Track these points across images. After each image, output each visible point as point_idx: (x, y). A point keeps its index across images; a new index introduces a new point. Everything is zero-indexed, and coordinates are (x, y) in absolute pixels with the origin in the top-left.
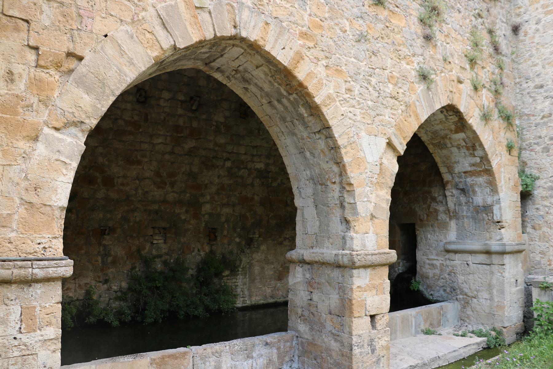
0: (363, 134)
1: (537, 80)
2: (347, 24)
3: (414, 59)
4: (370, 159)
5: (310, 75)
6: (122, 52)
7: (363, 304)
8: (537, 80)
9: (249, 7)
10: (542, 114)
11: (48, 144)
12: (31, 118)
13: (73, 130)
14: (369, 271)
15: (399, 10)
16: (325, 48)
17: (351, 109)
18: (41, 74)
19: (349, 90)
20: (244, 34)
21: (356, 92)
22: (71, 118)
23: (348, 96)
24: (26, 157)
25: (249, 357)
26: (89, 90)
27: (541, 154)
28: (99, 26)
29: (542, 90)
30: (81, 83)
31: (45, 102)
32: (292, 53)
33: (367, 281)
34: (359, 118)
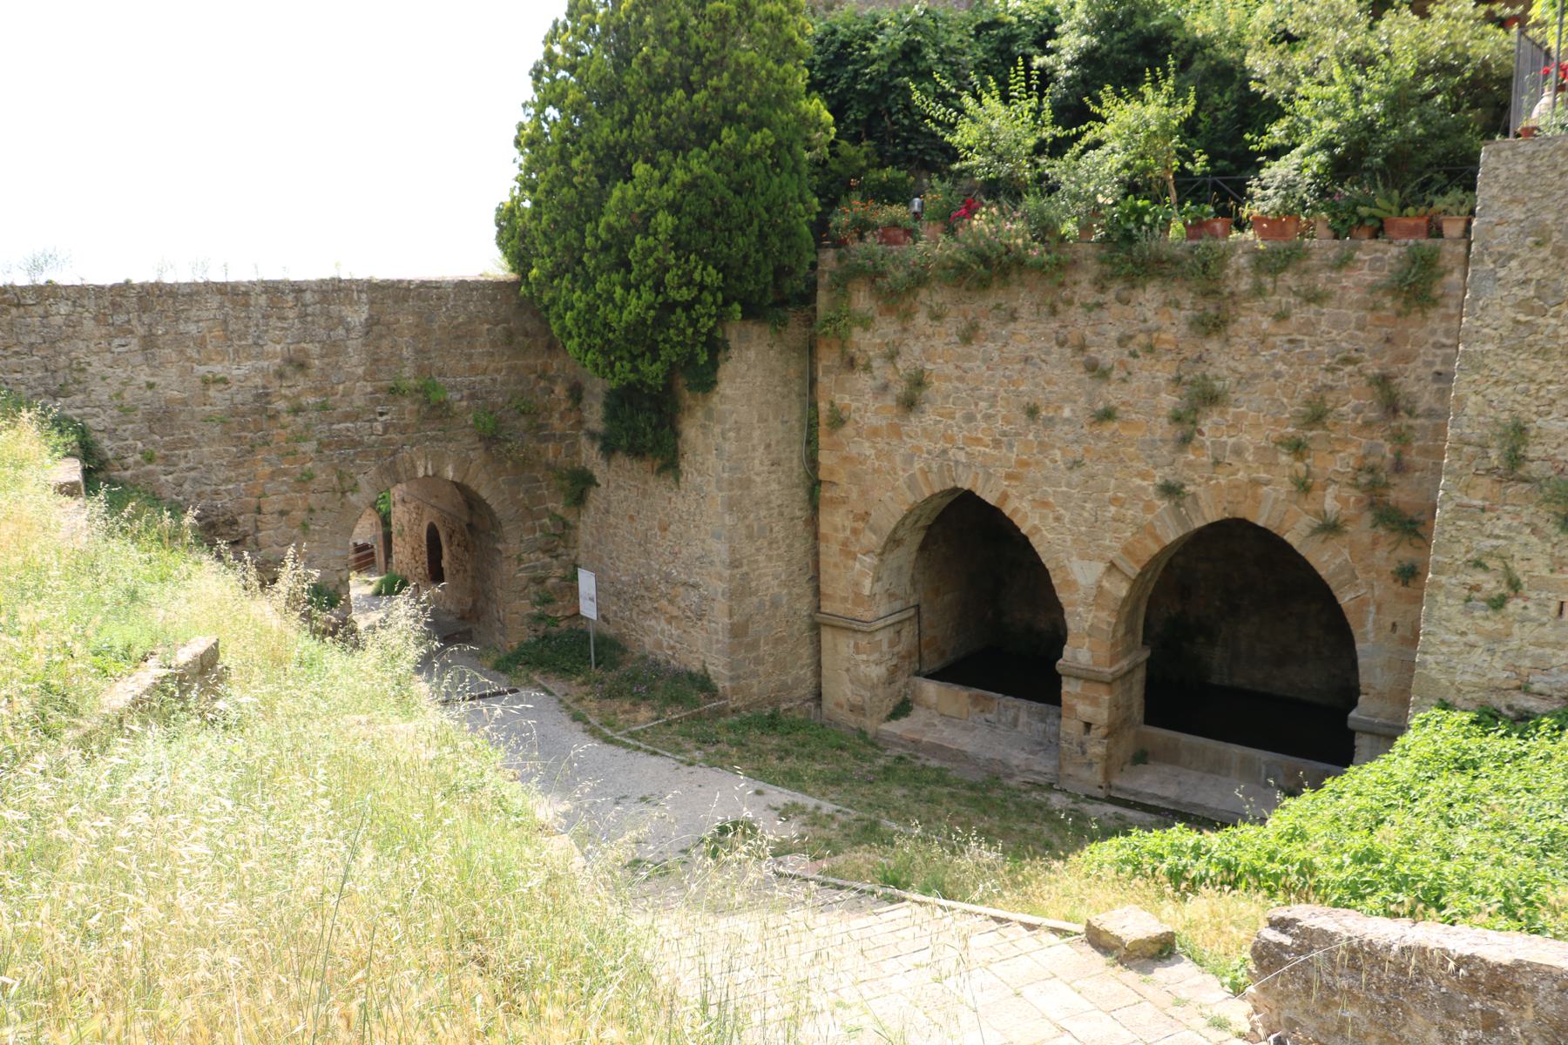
4: (1082, 581)
5: (1016, 510)
7: (1072, 708)
14: (1081, 682)
25: (1043, 721)
26: (875, 533)
33: (1079, 690)
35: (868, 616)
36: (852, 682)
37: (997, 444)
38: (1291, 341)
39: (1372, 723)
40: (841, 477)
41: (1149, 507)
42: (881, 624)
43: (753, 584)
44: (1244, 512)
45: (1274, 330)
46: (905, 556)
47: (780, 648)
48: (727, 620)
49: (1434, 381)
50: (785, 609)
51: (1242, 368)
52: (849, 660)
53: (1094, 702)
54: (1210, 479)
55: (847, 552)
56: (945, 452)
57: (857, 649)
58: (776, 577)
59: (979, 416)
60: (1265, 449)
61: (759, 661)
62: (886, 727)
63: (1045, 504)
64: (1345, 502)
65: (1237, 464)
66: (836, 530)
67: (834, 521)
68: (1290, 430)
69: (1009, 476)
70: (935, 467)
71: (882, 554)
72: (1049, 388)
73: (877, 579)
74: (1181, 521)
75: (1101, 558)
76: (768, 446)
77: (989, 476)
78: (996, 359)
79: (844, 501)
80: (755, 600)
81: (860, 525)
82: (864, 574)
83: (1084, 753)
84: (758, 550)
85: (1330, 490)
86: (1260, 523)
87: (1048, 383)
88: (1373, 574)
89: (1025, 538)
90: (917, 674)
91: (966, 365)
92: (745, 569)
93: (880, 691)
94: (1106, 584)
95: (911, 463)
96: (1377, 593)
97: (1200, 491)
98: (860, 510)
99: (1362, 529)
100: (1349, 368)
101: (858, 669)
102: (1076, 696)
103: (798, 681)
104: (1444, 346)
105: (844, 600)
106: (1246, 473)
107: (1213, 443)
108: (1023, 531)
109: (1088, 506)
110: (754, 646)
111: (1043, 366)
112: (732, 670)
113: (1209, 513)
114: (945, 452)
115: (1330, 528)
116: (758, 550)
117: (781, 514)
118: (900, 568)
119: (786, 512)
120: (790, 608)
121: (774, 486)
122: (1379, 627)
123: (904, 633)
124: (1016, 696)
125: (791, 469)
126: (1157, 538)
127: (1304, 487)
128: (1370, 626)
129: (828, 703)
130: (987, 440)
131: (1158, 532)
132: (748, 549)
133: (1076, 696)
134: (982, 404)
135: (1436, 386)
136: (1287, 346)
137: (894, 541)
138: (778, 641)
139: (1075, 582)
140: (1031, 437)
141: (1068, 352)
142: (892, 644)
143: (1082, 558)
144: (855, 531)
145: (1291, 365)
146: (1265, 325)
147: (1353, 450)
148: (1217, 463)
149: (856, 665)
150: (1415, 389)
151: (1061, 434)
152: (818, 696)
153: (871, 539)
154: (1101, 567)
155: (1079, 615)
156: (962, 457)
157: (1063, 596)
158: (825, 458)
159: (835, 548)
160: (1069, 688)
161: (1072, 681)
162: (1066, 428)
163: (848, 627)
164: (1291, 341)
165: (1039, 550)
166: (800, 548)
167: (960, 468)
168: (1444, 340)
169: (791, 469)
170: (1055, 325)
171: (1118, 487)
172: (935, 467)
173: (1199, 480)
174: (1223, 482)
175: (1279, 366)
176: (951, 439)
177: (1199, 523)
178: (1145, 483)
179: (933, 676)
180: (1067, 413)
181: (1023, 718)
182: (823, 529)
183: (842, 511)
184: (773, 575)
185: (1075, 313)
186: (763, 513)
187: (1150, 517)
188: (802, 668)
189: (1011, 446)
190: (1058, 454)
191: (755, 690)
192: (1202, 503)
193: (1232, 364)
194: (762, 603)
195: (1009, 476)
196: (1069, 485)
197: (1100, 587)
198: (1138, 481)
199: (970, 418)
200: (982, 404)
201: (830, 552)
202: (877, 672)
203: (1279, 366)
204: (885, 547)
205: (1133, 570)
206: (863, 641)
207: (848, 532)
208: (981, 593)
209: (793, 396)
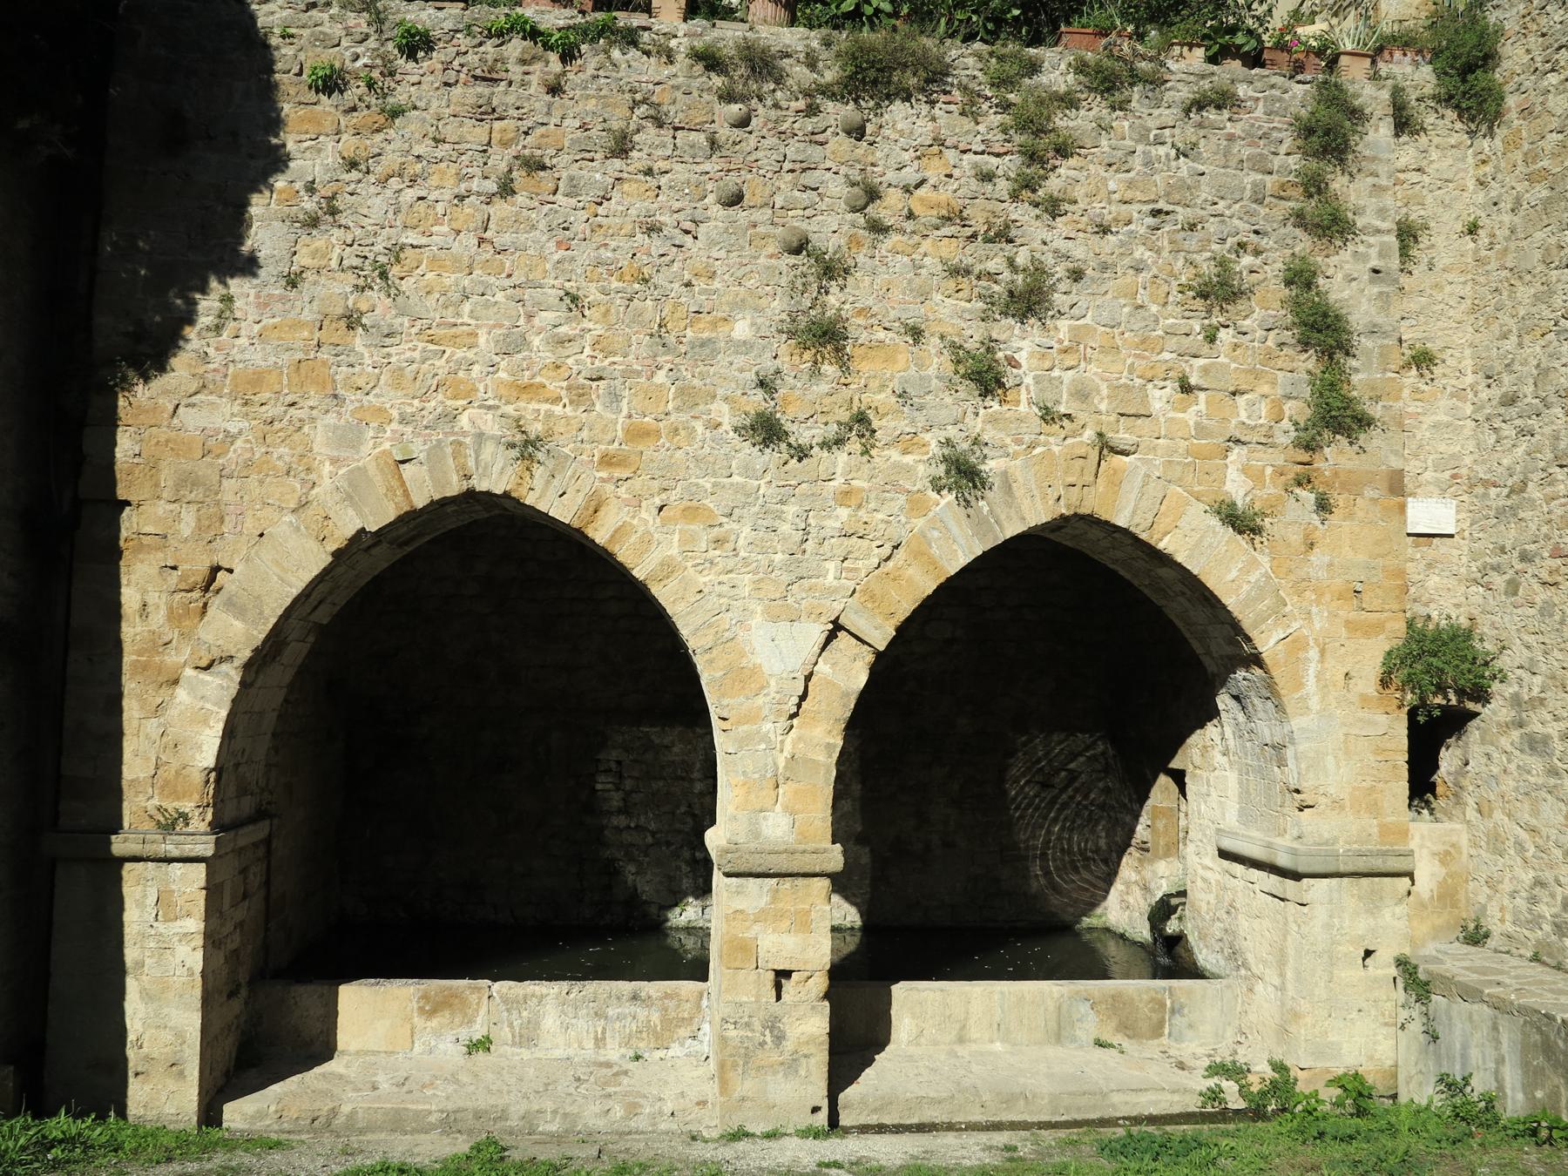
0: (757, 620)
1: (1506, 379)
2: (725, 408)
3: (927, 437)
5: (618, 533)
8: (1506, 379)
9: (492, 437)
10: (1509, 483)
11: (192, 690)
12: (172, 658)
13: (225, 667)
15: (890, 334)
16: (658, 474)
17: (723, 578)
19: (719, 542)
20: (482, 486)
21: (741, 542)
22: (216, 654)
23: (717, 552)
30: (231, 605)
32: (580, 499)
33: (764, 901)
37: (579, 396)
38: (1156, 213)
41: (916, 505)
44: (1095, 503)
49: (1372, 281)
54: (1032, 446)
59: (536, 341)
63: (692, 512)
68: (1166, 356)
69: (607, 461)
70: (418, 448)
74: (980, 525)
83: (779, 1038)
85: (1232, 456)
86: (1121, 521)
95: (355, 445)
96: (1317, 626)
104: (1378, 231)
107: (1037, 380)
108: (639, 573)
109: (791, 509)
113: (1032, 511)
130: (555, 386)
131: (935, 551)
135: (1376, 290)
136: (1150, 221)
139: (755, 671)
146: (1112, 185)
147: (1266, 389)
150: (1346, 294)
155: (765, 738)
162: (740, 360)
164: (1156, 213)
168: (1378, 223)
174: (1056, 449)
175: (1140, 252)
178: (909, 459)
180: (741, 329)
181: (550, 1021)
187: (919, 523)
189: (615, 397)
192: (1018, 491)
195: (607, 461)
198: (895, 455)
199: (512, 345)
203: (1140, 252)
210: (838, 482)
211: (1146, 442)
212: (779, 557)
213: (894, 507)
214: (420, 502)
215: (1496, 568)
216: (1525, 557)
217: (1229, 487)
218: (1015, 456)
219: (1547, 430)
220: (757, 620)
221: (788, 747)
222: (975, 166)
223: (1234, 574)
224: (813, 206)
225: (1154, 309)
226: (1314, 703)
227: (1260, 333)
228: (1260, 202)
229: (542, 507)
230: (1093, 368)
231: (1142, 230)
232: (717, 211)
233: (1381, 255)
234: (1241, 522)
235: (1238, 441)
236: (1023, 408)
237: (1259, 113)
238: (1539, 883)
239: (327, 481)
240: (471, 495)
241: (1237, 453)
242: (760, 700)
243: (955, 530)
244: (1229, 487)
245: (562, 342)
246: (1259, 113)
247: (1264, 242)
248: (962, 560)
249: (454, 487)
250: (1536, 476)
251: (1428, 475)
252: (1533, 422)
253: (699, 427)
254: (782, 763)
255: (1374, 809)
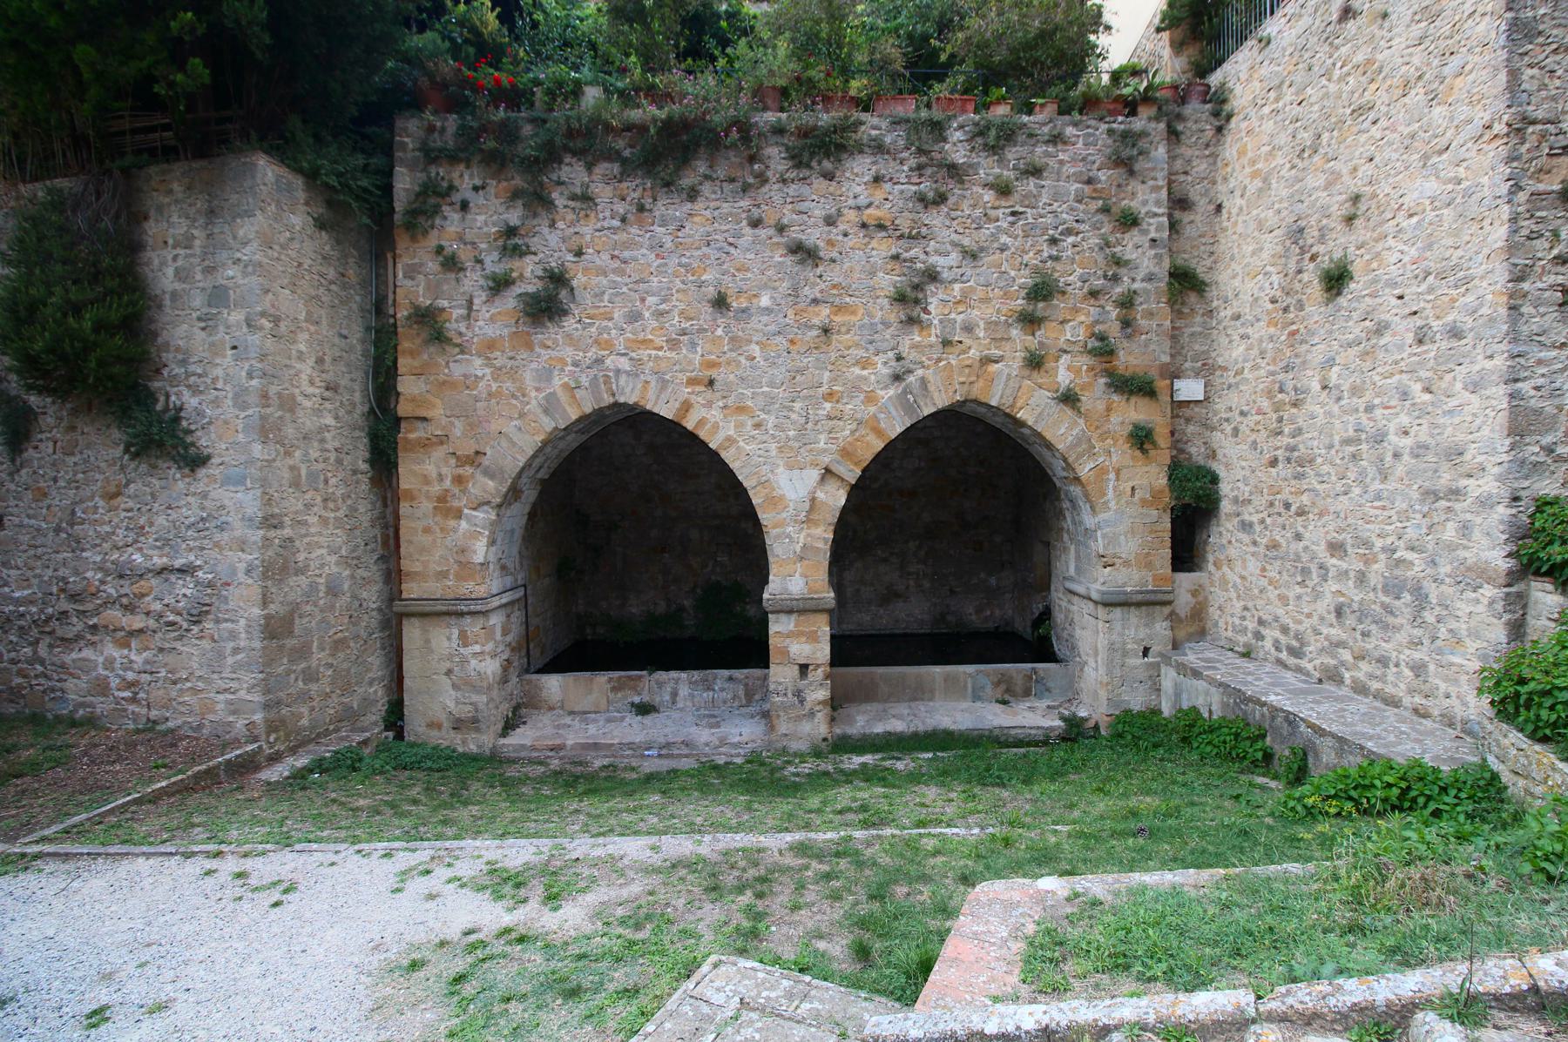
0: (781, 469)
2: (757, 348)
5: (702, 422)
6: (514, 444)
7: (785, 652)
11: (469, 519)
12: (456, 504)
14: (794, 617)
18: (460, 471)
19: (757, 426)
20: (622, 400)
24: (455, 530)
26: (492, 477)
27: (196, 629)
28: (494, 427)
29: (1238, 323)
31: (464, 491)
32: (677, 405)
33: (791, 627)
34: (774, 453)
35: (481, 591)
36: (455, 687)
37: (674, 344)
38: (1013, 214)
39: (1125, 593)
40: (437, 412)
42: (496, 602)
43: (301, 557)
44: (976, 392)
45: (997, 203)
46: (518, 514)
47: (341, 655)
48: (256, 611)
49: (1151, 247)
50: (346, 598)
51: (966, 242)
52: (450, 657)
53: (813, 637)
54: (939, 360)
55: (446, 508)
56: (599, 361)
57: (464, 640)
58: (333, 551)
59: (647, 315)
60: (996, 323)
61: (310, 676)
62: (502, 741)
63: (741, 409)
64: (1078, 372)
65: (967, 342)
66: (426, 480)
67: (421, 472)
70: (585, 381)
71: (499, 506)
72: (740, 276)
73: (492, 542)
75: (814, 465)
76: (320, 361)
77: (664, 384)
78: (669, 245)
79: (443, 440)
80: (303, 581)
81: (469, 470)
82: (475, 535)
84: (308, 506)
85: (1062, 361)
86: (993, 403)
87: (738, 270)
88: (1109, 441)
89: (715, 455)
90: (527, 671)
91: (626, 254)
92: (287, 532)
93: (495, 693)
94: (820, 495)
95: (549, 379)
96: (1114, 459)
97: (929, 374)
98: (468, 448)
99: (1096, 396)
100: (1071, 239)
101: (460, 668)
102: (790, 635)
103: (367, 702)
104: (1156, 215)
105: (443, 575)
106: (970, 354)
107: (941, 322)
109: (797, 405)
110: (303, 652)
111: (732, 250)
112: (267, 691)
114: (599, 361)
115: (1069, 399)
116: (308, 506)
117: (339, 462)
118: (512, 531)
119: (347, 460)
120: (354, 597)
121: (329, 421)
122: (1119, 495)
123: (513, 619)
124: (667, 668)
125: (353, 405)
126: (878, 432)
127: (1035, 362)
128: (1110, 494)
129: (415, 725)
130: (659, 341)
131: (883, 425)
132: (294, 503)
133: (790, 635)
134: (651, 300)
136: (1011, 219)
137: (514, 492)
138: (339, 645)
139: (782, 498)
140: (719, 332)
141: (762, 233)
142: (505, 632)
143: (790, 468)
144: (459, 480)
145: (1016, 237)
146: (986, 198)
147: (1083, 318)
148: (946, 343)
149: (464, 661)
151: (760, 326)
152: (395, 717)
153: (490, 487)
154: (814, 474)
155: (789, 536)
156: (624, 363)
157: (764, 517)
158: (408, 386)
159: (427, 506)
160: (778, 627)
161: (783, 617)
162: (765, 319)
163: (451, 612)
164: (1013, 214)
165: (734, 466)
166: (365, 511)
167: (623, 379)
169: (353, 405)
170: (745, 203)
171: (833, 380)
172: (585, 381)
173: (927, 363)
175: (1004, 239)
176: (608, 345)
177: (927, 412)
178: (865, 373)
179: (556, 665)
180: (765, 301)
182: (406, 482)
183: (439, 452)
184: (328, 548)
185: (772, 191)
186: (314, 454)
187: (872, 409)
188: (371, 684)
189: (693, 345)
190: (756, 350)
191: (305, 722)
192: (931, 388)
193: (955, 237)
194: (313, 587)
195: (692, 382)
196: (771, 384)
197: (813, 500)
198: (857, 371)
199: (634, 317)
200: (651, 300)
201: (416, 518)
202: (491, 667)
203: (1004, 239)
204: (506, 496)
205: (852, 474)
206: (473, 627)
207: (448, 483)
208: (632, 548)
209: (355, 306)
210: (825, 389)
211: (1007, 354)
212: (791, 433)
213: (857, 401)
214: (588, 410)
215: (1227, 420)
216: (1242, 413)
217: (1060, 379)
218: (928, 368)
219: (1256, 336)
220: (781, 469)
221: (802, 540)
222: (902, 192)
223: (1063, 431)
224: (804, 223)
225: (1013, 273)
226: (1112, 504)
227: (1079, 284)
228: (1080, 202)
229: (656, 410)
230: (976, 312)
231: (1005, 225)
232: (748, 230)
233: (1157, 230)
234: (1069, 399)
235: (1065, 352)
236: (933, 339)
237: (1080, 145)
238: (1246, 608)
239: (534, 402)
240: (616, 404)
241: (1065, 360)
242: (784, 515)
243: (894, 413)
244: (1060, 379)
245: (661, 314)
246: (1080, 145)
247: (1082, 227)
248: (899, 430)
249: (608, 400)
250: (1248, 365)
251: (1187, 365)
252: (1250, 331)
253: (742, 359)
254: (798, 549)
255: (1149, 566)
